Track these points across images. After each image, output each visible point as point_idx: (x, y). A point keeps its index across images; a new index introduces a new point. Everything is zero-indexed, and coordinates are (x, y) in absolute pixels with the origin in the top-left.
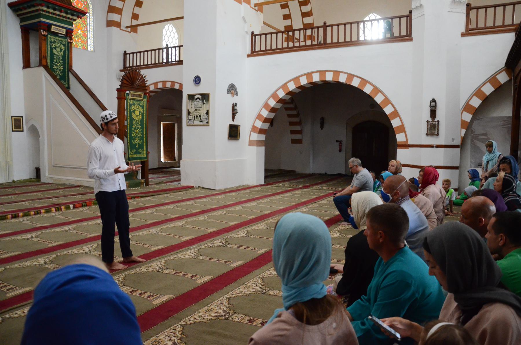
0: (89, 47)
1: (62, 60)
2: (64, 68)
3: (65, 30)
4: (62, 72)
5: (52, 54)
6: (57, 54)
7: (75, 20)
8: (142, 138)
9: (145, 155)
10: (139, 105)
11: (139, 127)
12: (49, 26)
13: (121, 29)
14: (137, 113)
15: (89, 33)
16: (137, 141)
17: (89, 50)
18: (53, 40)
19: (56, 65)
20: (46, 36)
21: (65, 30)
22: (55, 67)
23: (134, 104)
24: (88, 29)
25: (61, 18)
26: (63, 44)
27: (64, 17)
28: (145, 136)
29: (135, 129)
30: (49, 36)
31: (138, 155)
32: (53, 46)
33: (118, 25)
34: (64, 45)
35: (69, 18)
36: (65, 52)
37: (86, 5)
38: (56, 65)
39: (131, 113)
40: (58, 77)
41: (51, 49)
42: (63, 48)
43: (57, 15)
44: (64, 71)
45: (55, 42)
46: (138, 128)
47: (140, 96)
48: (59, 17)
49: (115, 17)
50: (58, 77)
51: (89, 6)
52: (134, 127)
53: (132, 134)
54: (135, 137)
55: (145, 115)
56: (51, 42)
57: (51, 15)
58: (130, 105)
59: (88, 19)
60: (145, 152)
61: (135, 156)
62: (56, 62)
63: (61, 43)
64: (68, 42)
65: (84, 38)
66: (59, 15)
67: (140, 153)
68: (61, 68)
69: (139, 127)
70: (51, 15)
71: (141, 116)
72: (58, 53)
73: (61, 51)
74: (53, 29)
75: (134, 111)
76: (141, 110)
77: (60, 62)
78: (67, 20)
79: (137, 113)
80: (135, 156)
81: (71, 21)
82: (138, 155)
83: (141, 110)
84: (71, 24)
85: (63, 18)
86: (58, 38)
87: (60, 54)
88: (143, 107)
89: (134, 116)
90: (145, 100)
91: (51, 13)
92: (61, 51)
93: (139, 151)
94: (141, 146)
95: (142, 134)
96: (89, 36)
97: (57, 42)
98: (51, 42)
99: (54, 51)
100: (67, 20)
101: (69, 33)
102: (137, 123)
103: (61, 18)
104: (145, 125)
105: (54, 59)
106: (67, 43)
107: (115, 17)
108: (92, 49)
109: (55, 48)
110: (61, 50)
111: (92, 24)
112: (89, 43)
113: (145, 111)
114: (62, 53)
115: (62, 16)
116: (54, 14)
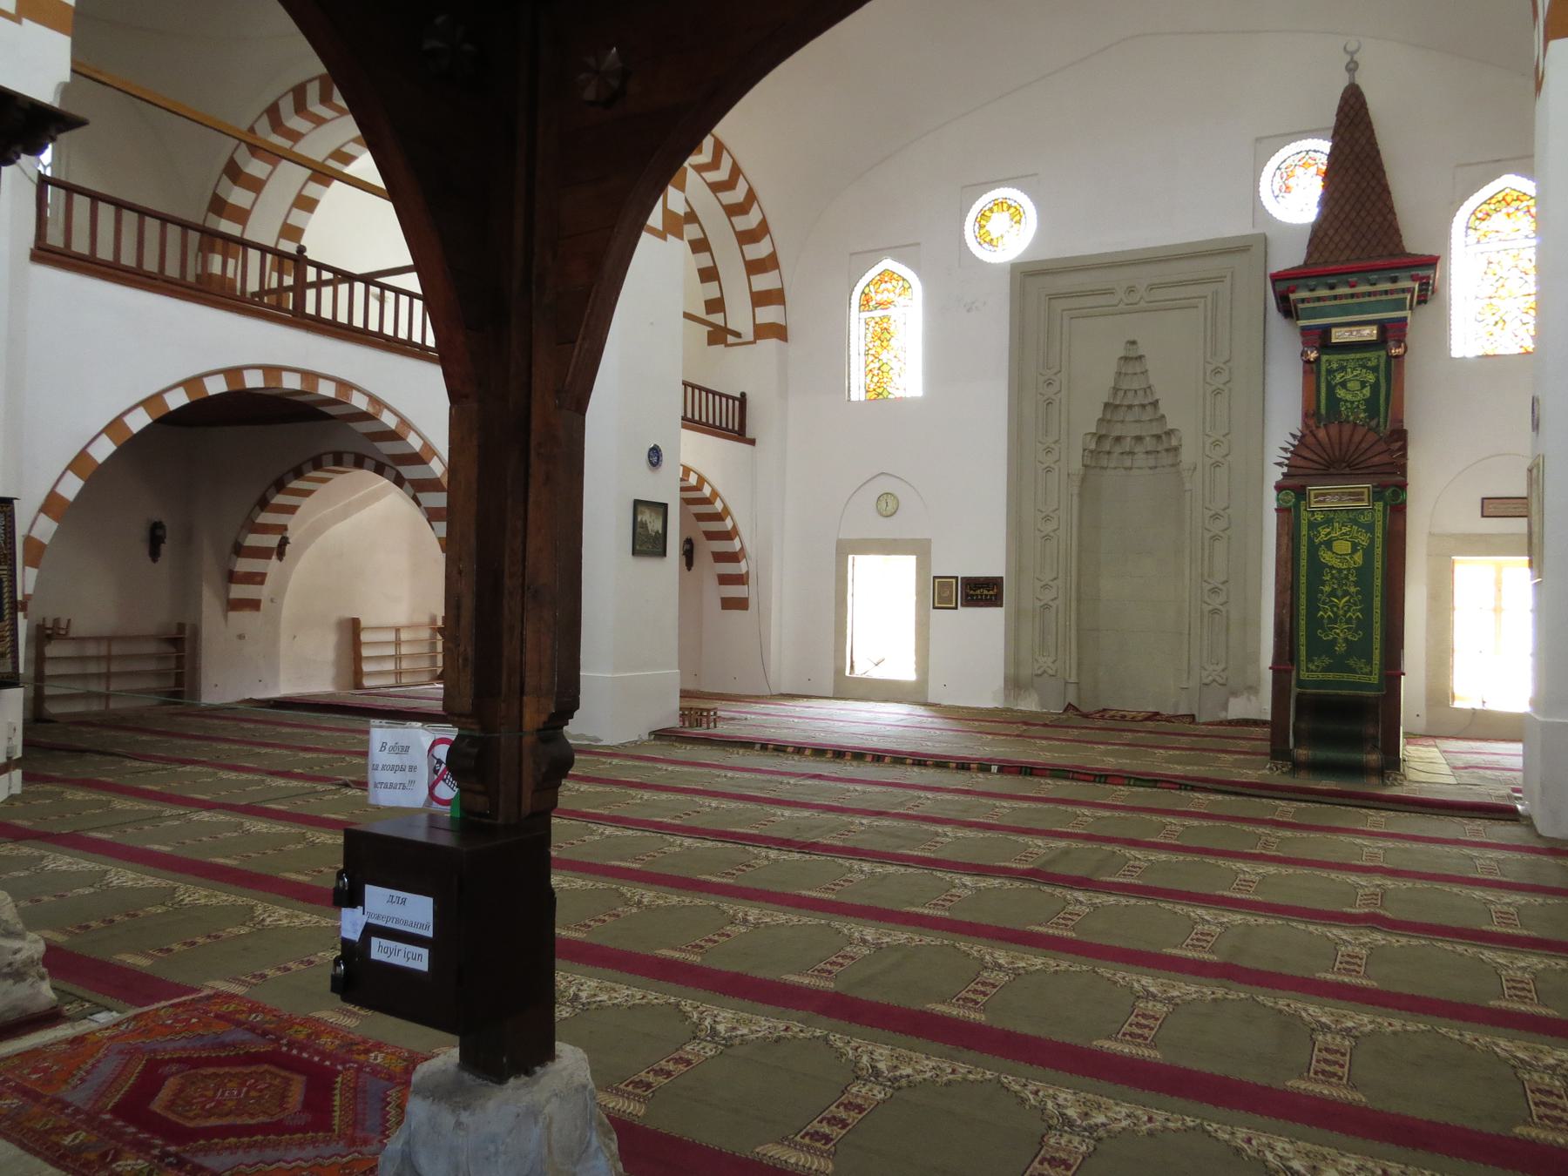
6: (1349, 397)
8: (1365, 624)
9: (1375, 679)
10: (1355, 522)
11: (1353, 589)
12: (1326, 331)
14: (1343, 547)
16: (1340, 632)
18: (1335, 366)
20: (1317, 360)
23: (1328, 522)
27: (1370, 294)
28: (1377, 617)
29: (1333, 593)
30: (1324, 358)
31: (1346, 677)
32: (1339, 377)
34: (1375, 369)
35: (1386, 292)
36: (1375, 388)
39: (1313, 550)
41: (1331, 390)
42: (1371, 378)
45: (1342, 369)
46: (1346, 593)
47: (1357, 496)
52: (1327, 589)
53: (1319, 609)
54: (1333, 621)
55: (1378, 551)
56: (1330, 372)
58: (1313, 526)
60: (1376, 669)
61: (1331, 676)
63: (1364, 366)
64: (1389, 357)
67: (1353, 671)
69: (1353, 589)
70: (1328, 303)
71: (1358, 557)
72: (1353, 393)
74: (1339, 336)
75: (1329, 544)
76: (1364, 540)
79: (1343, 547)
80: (1331, 676)
82: (1346, 677)
83: (1364, 540)
86: (1352, 356)
87: (1360, 397)
88: (1370, 528)
89: (1326, 557)
90: (1379, 506)
93: (1351, 662)
94: (1361, 649)
95: (1367, 611)
98: (1330, 372)
99: (1341, 393)
100: (1384, 297)
102: (1341, 577)
104: (1378, 582)
106: (1383, 361)
109: (1343, 385)
110: (1363, 384)
113: (1379, 542)
114: (1367, 392)
115: (1363, 295)
116: (1335, 297)
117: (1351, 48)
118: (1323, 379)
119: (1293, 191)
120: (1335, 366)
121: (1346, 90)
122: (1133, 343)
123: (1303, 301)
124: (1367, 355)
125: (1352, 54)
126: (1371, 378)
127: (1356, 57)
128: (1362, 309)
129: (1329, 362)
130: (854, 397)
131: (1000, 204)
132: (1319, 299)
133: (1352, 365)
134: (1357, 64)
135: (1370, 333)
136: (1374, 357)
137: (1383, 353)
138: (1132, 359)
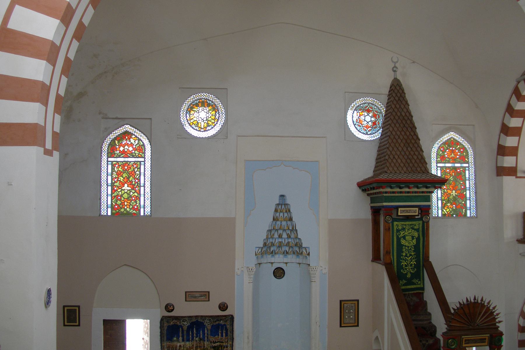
0: (468, 212)
1: (414, 251)
2: (418, 261)
3: (417, 209)
4: (415, 267)
5: (400, 246)
6: (407, 244)
7: (432, 192)
13: (517, 177)
15: (468, 192)
17: (468, 215)
18: (400, 228)
19: (406, 260)
21: (417, 209)
22: (404, 263)
24: (467, 186)
25: (412, 195)
26: (415, 229)
27: (416, 192)
30: (395, 223)
32: (402, 235)
33: (512, 171)
34: (417, 230)
35: (423, 192)
36: (418, 239)
37: (462, 152)
38: (406, 260)
40: (409, 276)
41: (399, 239)
42: (416, 235)
43: (405, 192)
44: (417, 266)
45: (404, 229)
48: (409, 194)
49: (508, 161)
50: (409, 276)
51: (468, 152)
56: (398, 231)
57: (397, 195)
59: (467, 172)
62: (406, 256)
63: (413, 228)
65: (460, 201)
66: (408, 192)
68: (414, 262)
70: (397, 195)
72: (408, 242)
73: (413, 239)
77: (411, 255)
78: (421, 194)
81: (428, 194)
84: (428, 199)
85: (414, 194)
86: (407, 223)
91: (398, 192)
92: (413, 239)
96: (468, 196)
97: (407, 227)
98: (398, 231)
99: (403, 242)
100: (421, 194)
101: (426, 211)
103: (412, 195)
105: (403, 252)
106: (421, 226)
107: (508, 161)
108: (474, 214)
109: (404, 237)
110: (413, 237)
111: (472, 177)
112: (468, 205)
114: (414, 241)
115: (413, 192)
116: (401, 192)
117: (395, 60)
118: (395, 234)
119: (362, 125)
120: (400, 228)
121: (393, 81)
122: (282, 196)
123: (386, 193)
124: (414, 223)
125: (395, 63)
126: (416, 235)
127: (397, 65)
128: (410, 199)
129: (397, 225)
130: (103, 213)
131: (204, 103)
132: (393, 192)
133: (407, 227)
134: (397, 68)
135: (415, 212)
136: (418, 224)
137: (421, 222)
138: (283, 207)
